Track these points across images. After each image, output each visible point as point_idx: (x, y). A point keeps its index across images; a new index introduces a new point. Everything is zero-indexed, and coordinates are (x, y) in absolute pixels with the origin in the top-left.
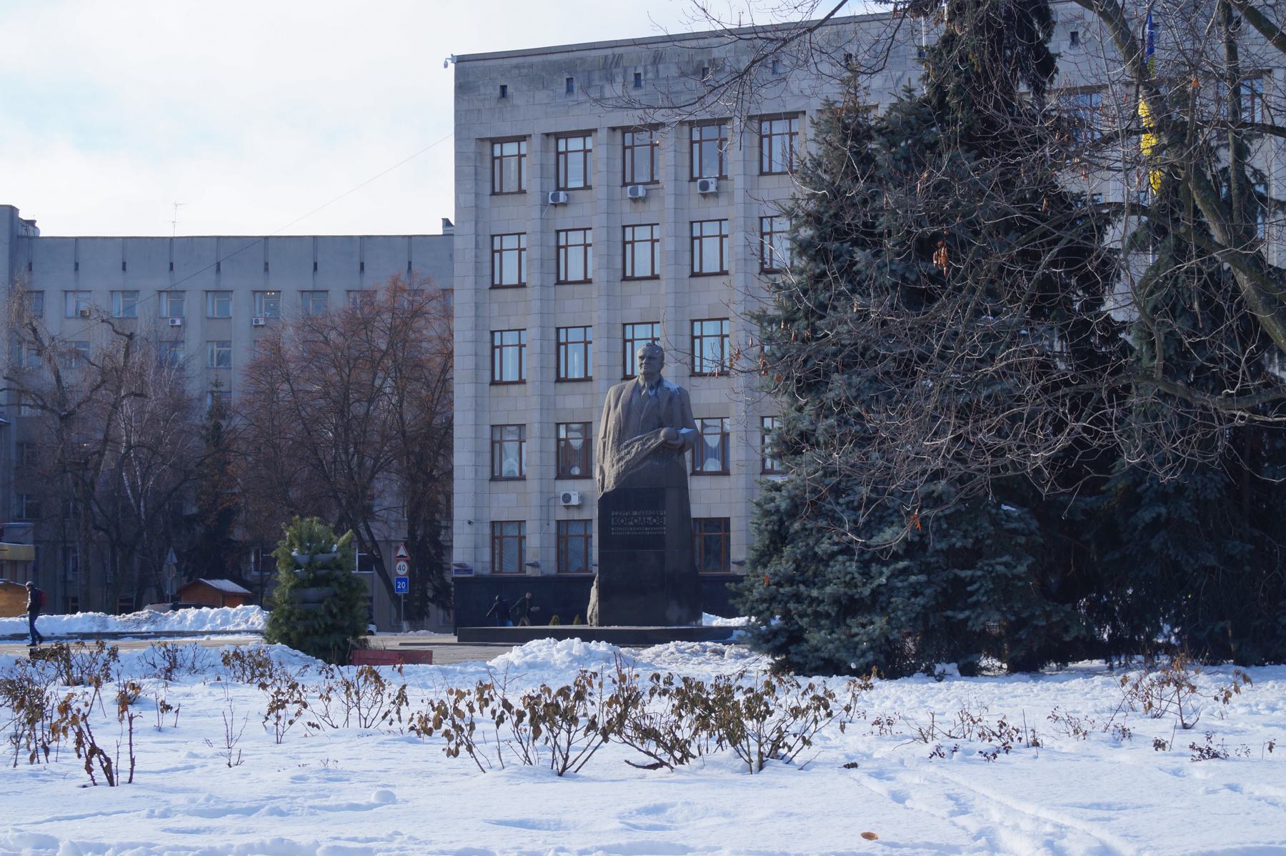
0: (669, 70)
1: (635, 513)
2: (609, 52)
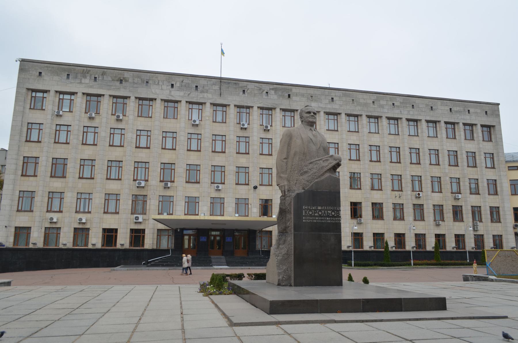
1: (319, 208)
2: (85, 68)
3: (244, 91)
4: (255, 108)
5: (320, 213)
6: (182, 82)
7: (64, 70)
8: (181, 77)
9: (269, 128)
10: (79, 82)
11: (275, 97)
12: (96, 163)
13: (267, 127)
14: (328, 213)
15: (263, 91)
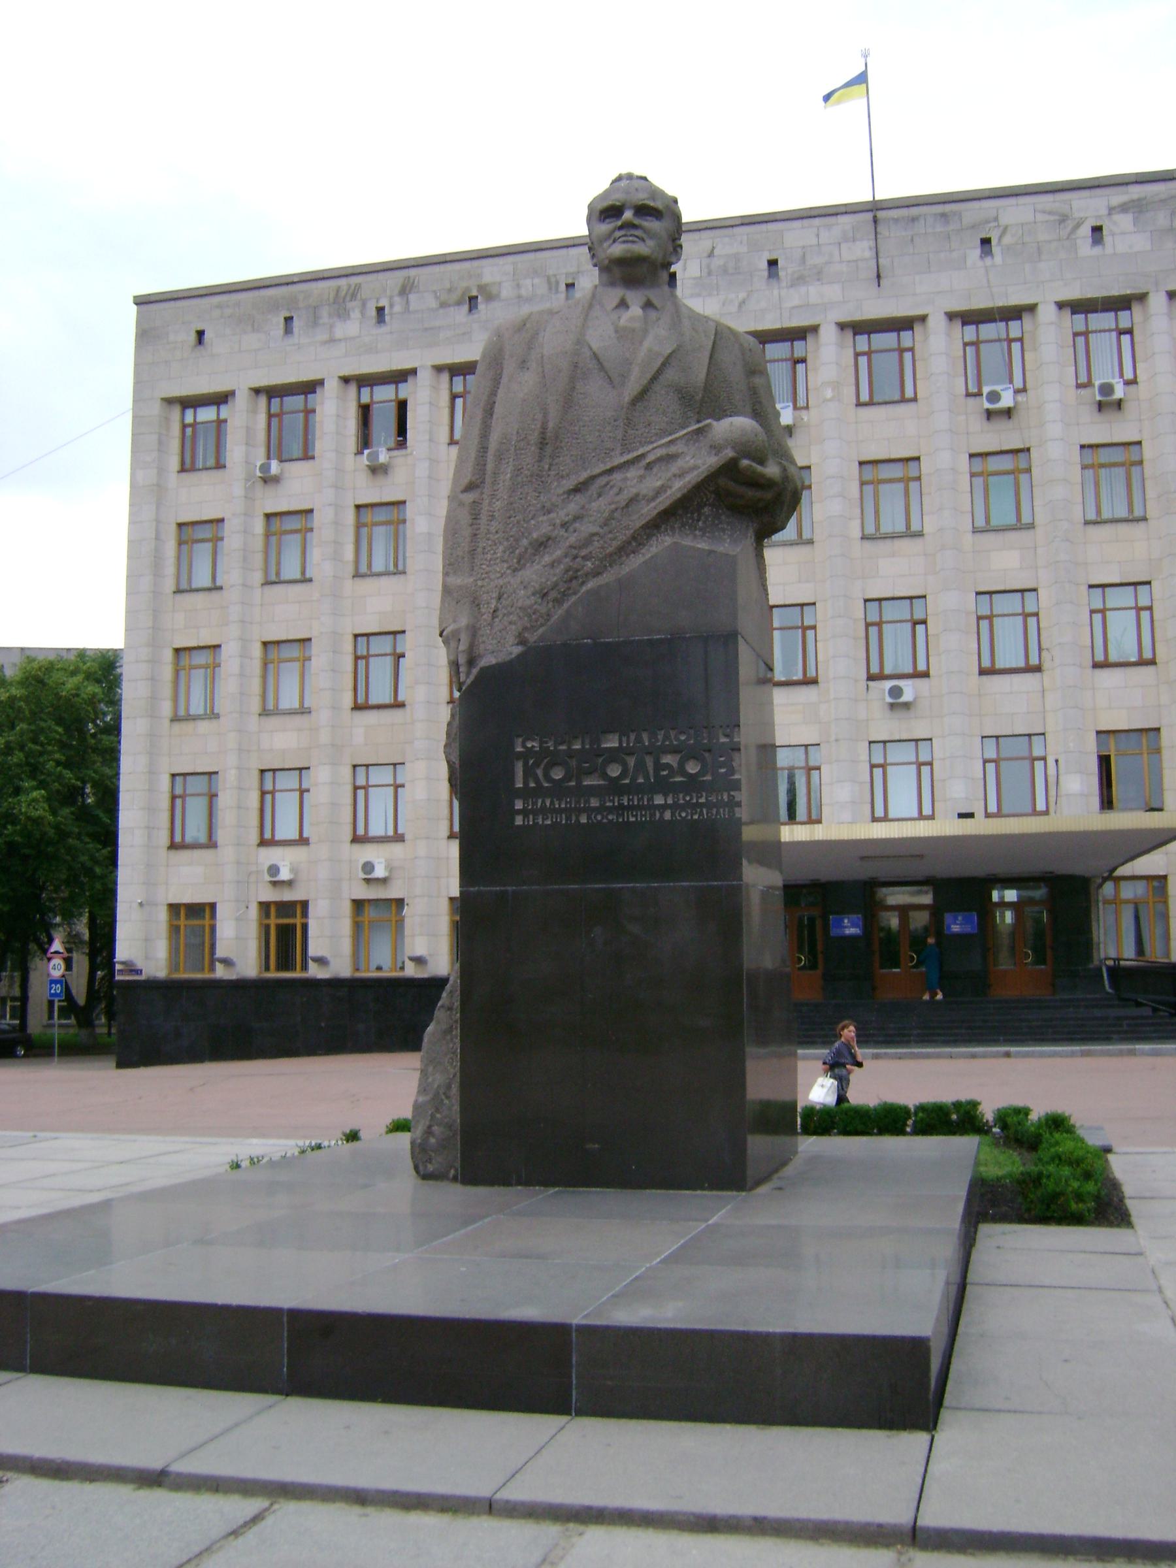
0: (423, 301)
1: (611, 742)
2: (343, 282)
3: (986, 242)
4: (1047, 312)
5: (614, 771)
6: (711, 255)
7: (274, 306)
8: (705, 234)
9: (1119, 392)
10: (326, 337)
11: (1140, 242)
12: (407, 645)
13: (1107, 389)
14: (658, 767)
15: (1078, 226)
